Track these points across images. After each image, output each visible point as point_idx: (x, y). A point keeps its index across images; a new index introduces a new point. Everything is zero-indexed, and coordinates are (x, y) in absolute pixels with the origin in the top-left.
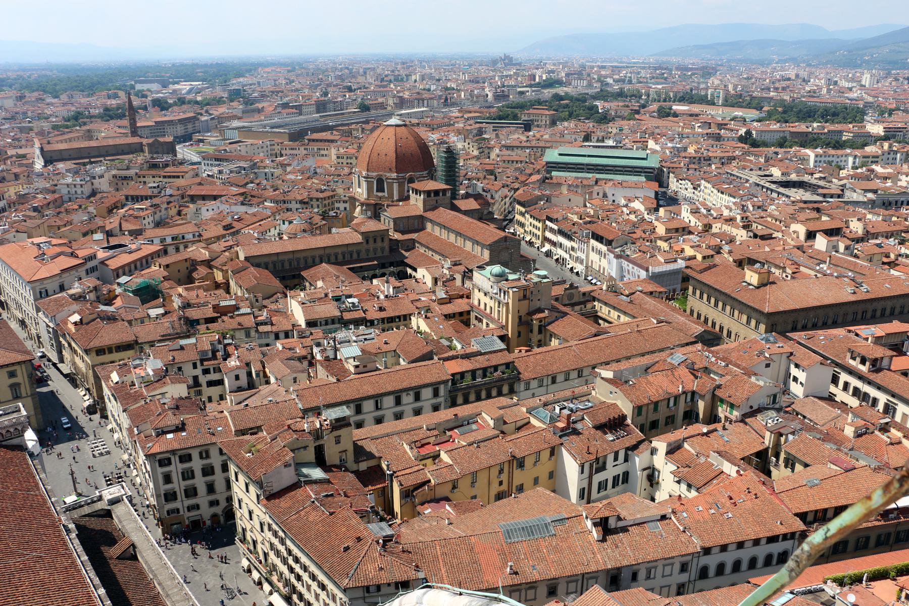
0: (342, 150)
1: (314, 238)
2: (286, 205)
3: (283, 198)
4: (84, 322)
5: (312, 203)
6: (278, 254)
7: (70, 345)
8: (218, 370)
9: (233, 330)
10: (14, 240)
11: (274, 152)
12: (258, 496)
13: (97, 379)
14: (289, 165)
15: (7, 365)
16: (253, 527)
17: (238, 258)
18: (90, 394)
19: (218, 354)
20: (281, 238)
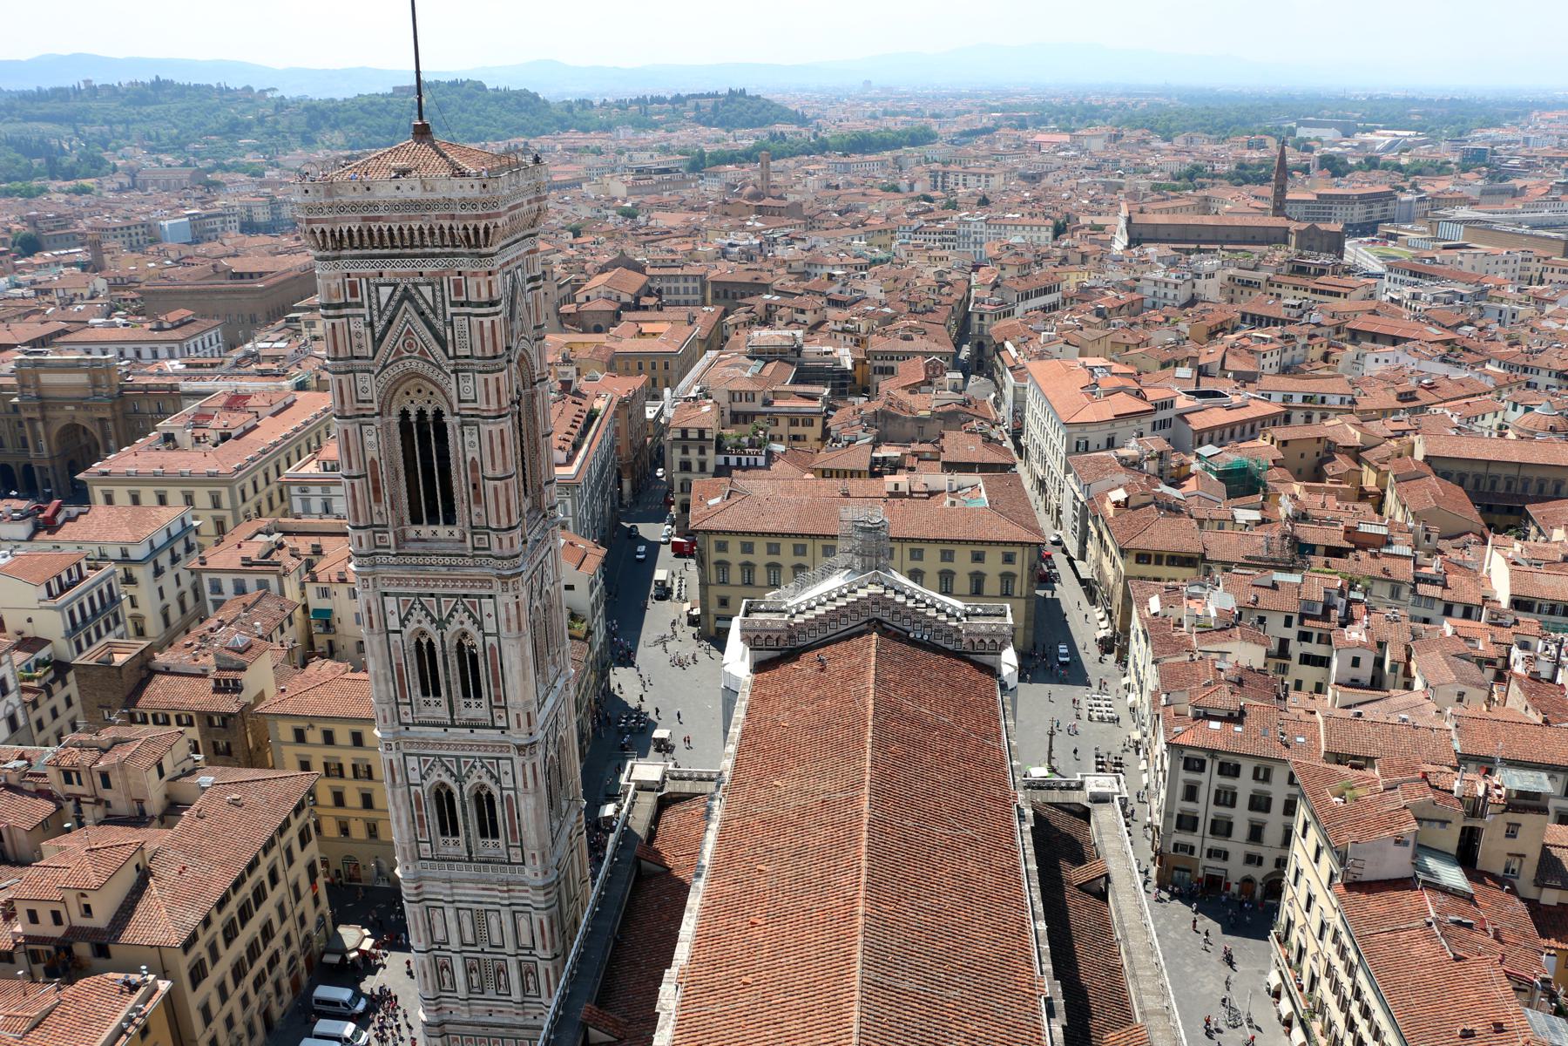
2: (1528, 376)
3: (1524, 362)
6: (1489, 462)
7: (1100, 535)
8: (1325, 639)
9: (1373, 579)
10: (1060, 355)
11: (1529, 274)
12: (1332, 875)
13: (1127, 599)
14: (1553, 301)
15: (1006, 543)
16: (1307, 924)
17: (1412, 455)
18: (1111, 621)
19: (1333, 612)
20: (1502, 435)
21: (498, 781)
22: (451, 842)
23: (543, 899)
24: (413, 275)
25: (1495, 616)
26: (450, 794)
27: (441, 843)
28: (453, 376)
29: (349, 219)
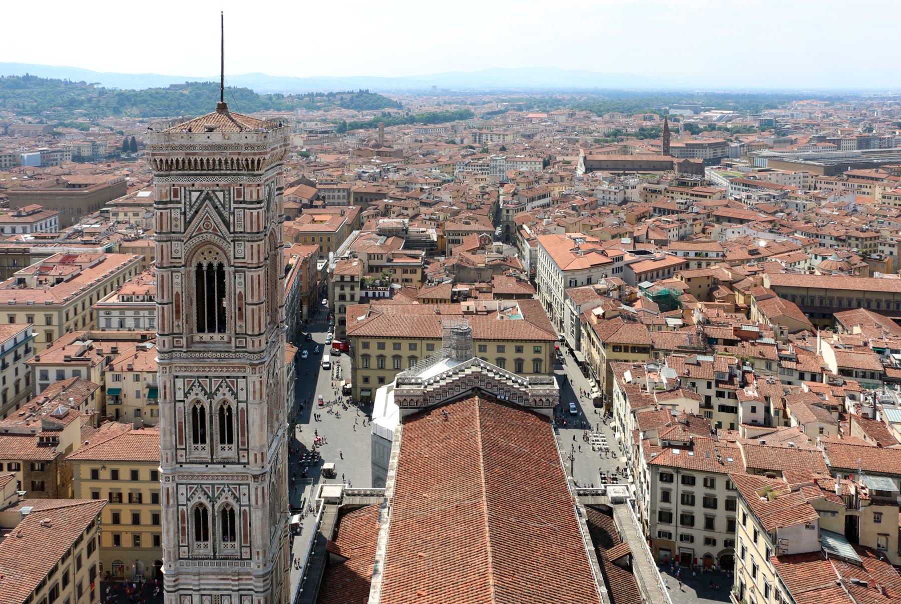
0: (888, 190)
1: (852, 279)
2: (819, 240)
3: (816, 232)
4: (607, 316)
5: (850, 241)
6: (808, 288)
7: (589, 335)
8: (733, 396)
9: (754, 358)
11: (808, 184)
13: (610, 373)
14: (825, 199)
17: (763, 285)
18: (600, 387)
19: (735, 379)
20: (812, 273)
21: (238, 500)
22: (202, 546)
23: (261, 584)
24: (213, 185)
25: (831, 379)
26: (205, 511)
27: (195, 546)
28: (232, 243)
29: (177, 154)
